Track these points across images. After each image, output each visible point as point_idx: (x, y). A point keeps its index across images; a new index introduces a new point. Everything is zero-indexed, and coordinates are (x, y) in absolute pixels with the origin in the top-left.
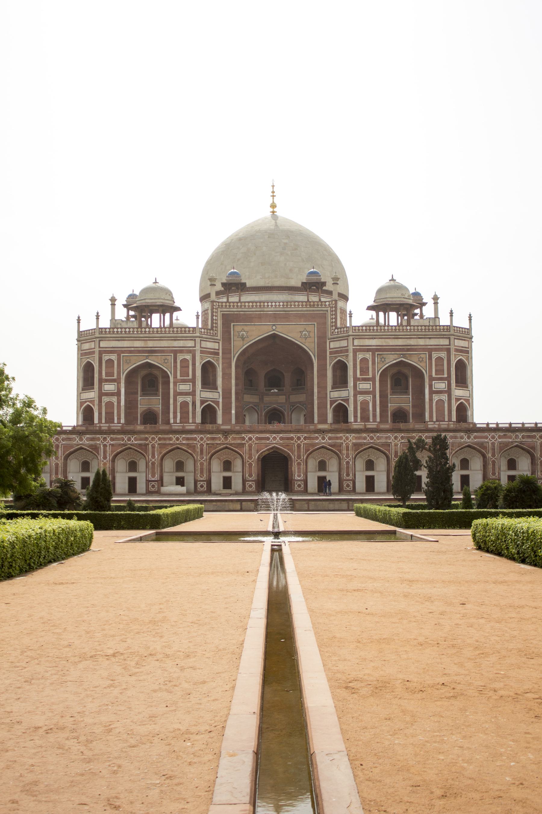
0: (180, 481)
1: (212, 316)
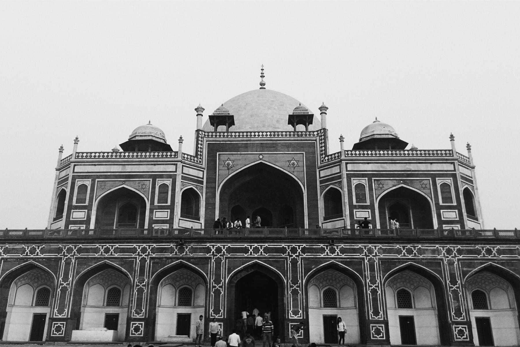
0: (111, 322)
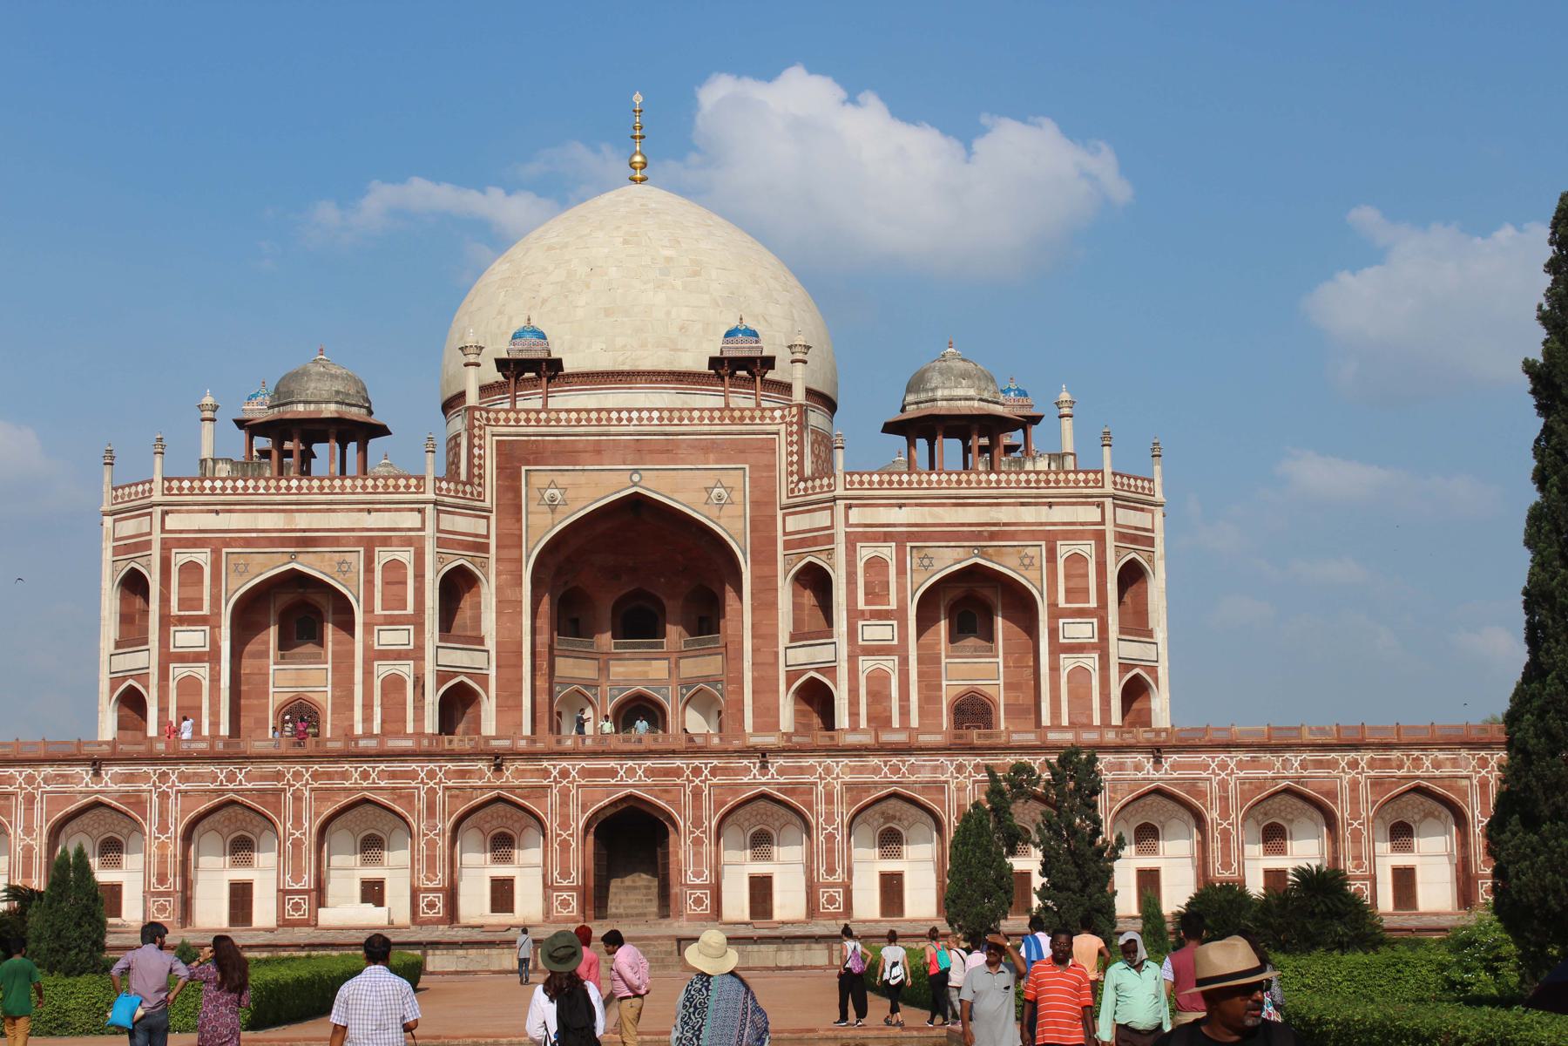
0: (373, 892)
1: (471, 446)
